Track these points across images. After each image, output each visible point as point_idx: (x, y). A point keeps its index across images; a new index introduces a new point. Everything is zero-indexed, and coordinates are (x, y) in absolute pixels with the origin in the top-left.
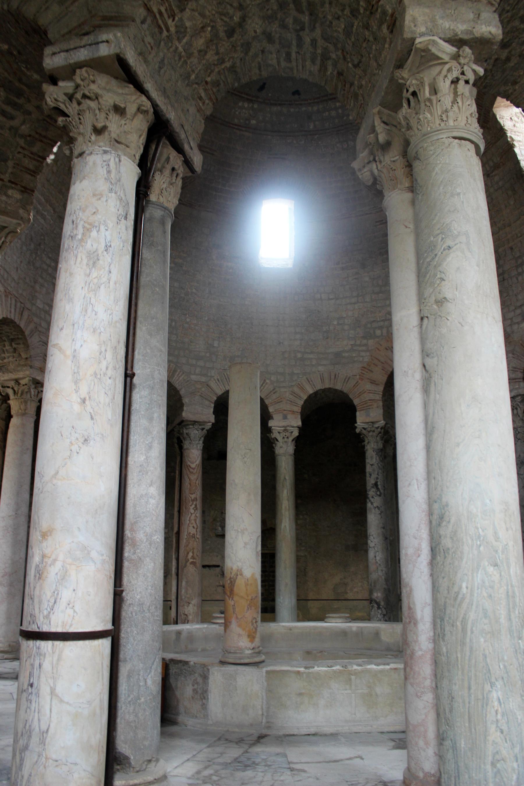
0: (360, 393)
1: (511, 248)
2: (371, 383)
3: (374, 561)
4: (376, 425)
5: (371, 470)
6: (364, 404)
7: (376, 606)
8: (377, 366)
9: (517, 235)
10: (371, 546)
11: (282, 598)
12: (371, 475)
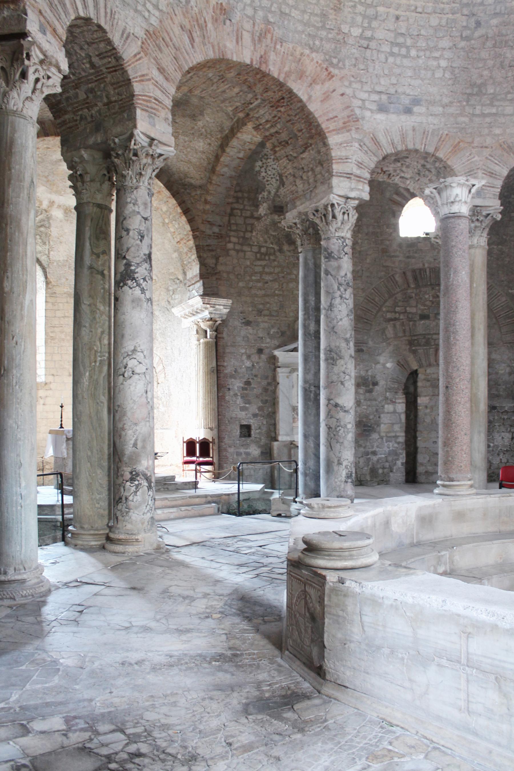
0: (143, 75)
1: (397, 18)
2: (158, 68)
3: (144, 400)
4: (159, 151)
5: (142, 228)
6: (147, 101)
7: (146, 484)
8: (167, 46)
9: (416, 8)
10: (137, 370)
11: (23, 484)
12: (143, 237)
